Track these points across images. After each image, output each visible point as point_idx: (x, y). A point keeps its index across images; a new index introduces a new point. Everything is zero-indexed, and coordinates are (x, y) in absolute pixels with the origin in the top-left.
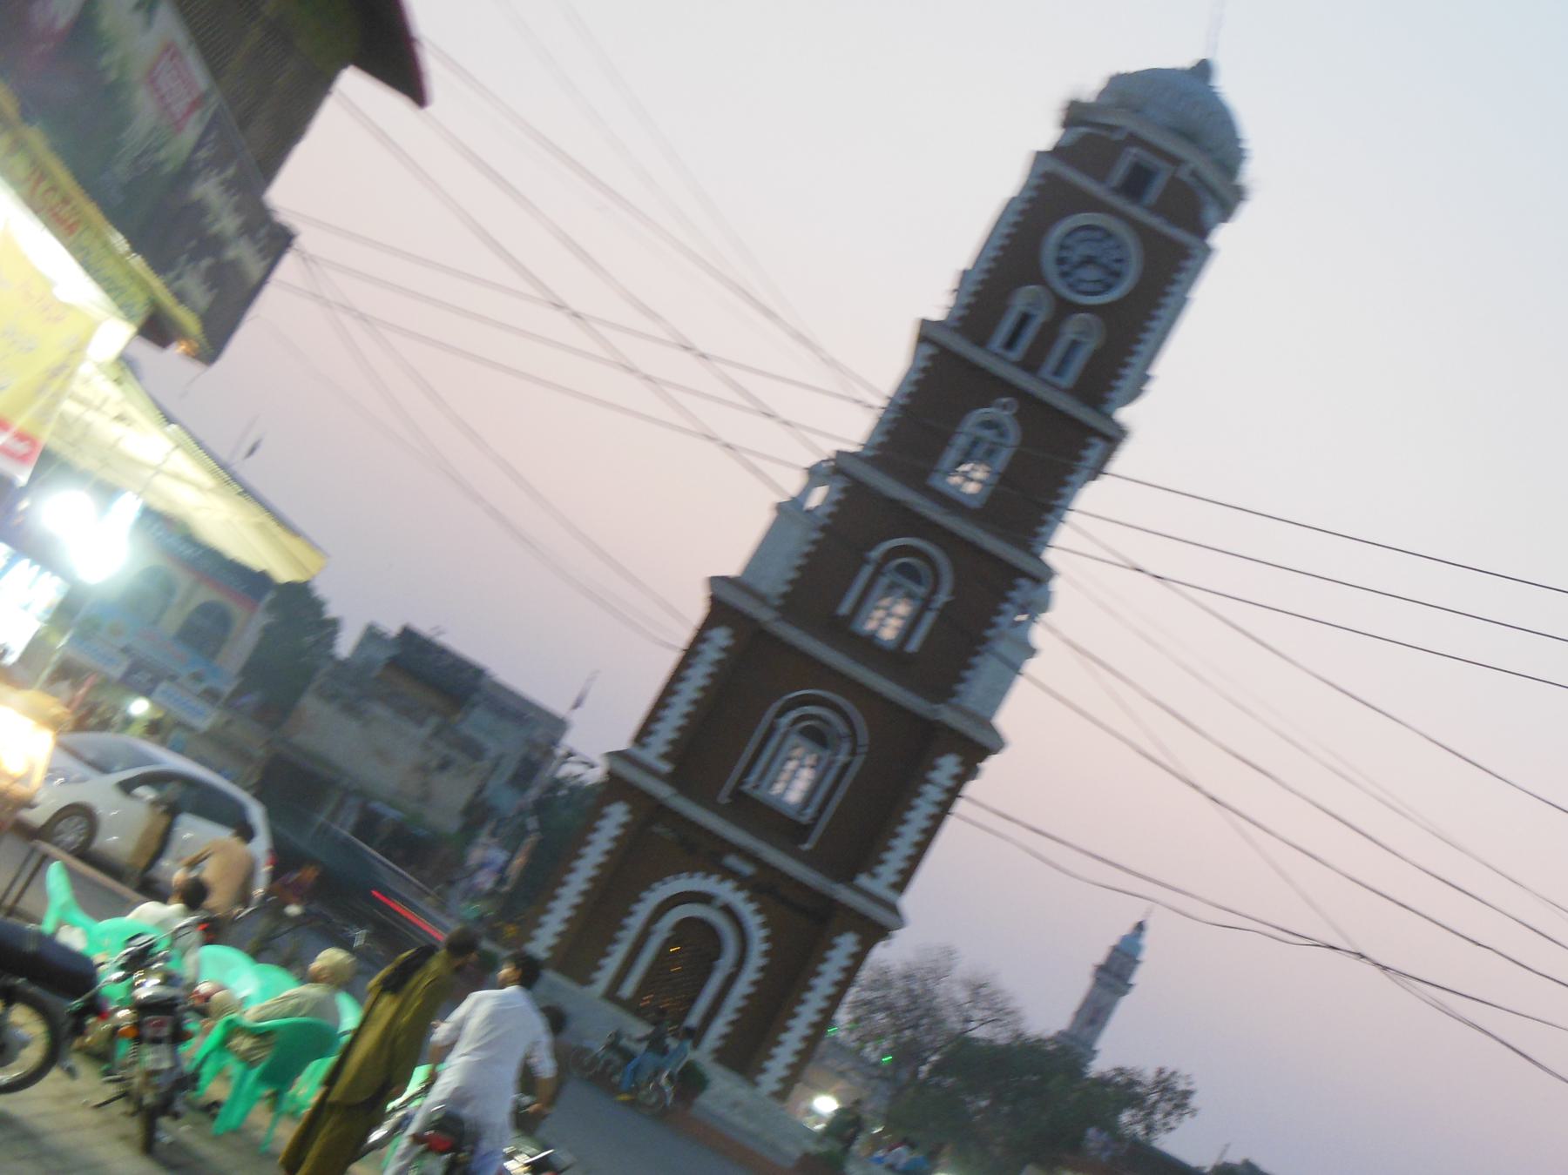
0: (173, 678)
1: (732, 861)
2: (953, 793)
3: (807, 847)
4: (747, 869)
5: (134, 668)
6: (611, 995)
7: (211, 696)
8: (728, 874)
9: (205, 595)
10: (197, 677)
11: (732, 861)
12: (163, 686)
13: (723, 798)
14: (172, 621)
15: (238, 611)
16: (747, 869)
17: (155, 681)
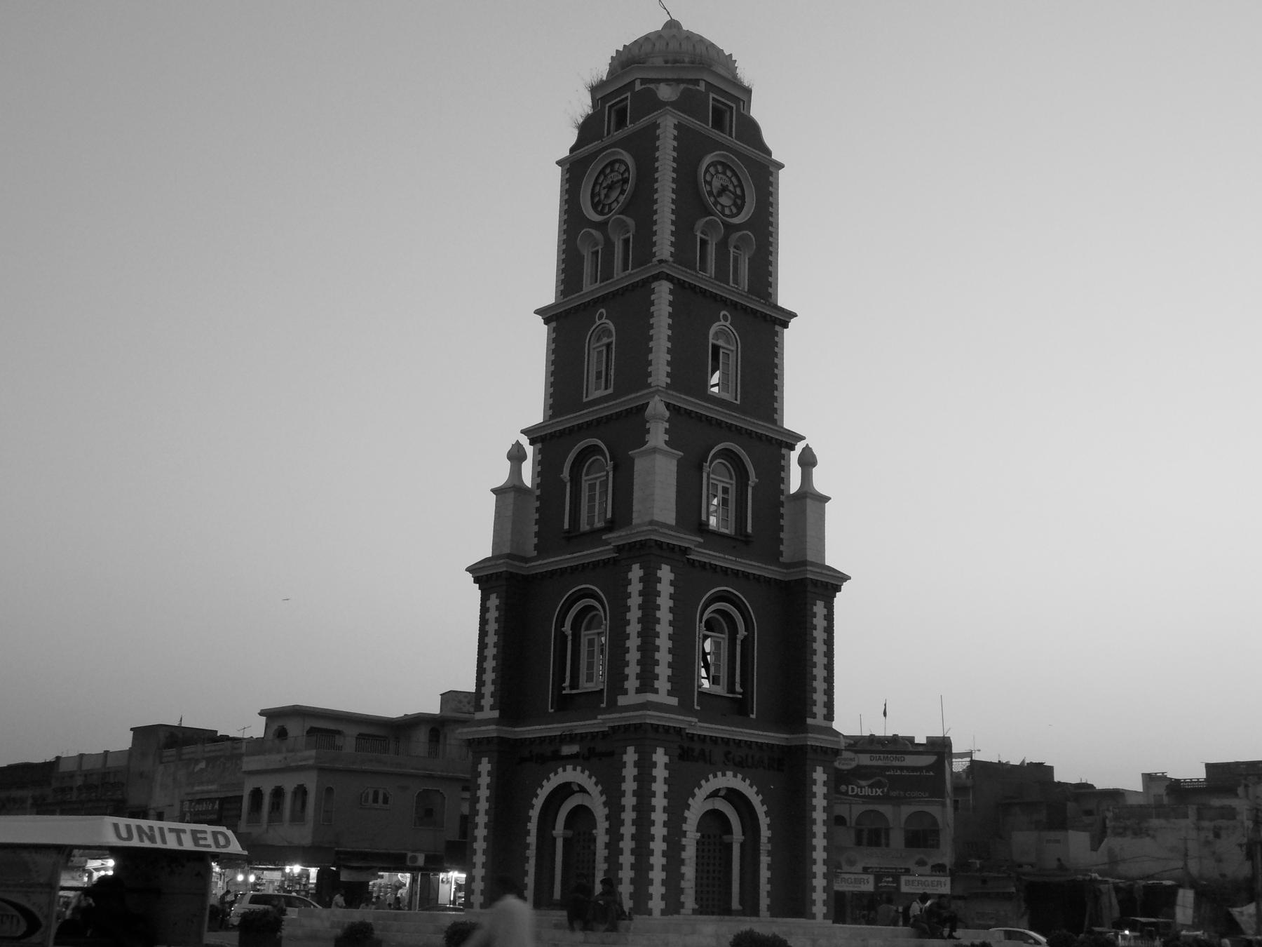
0: (907, 871)
1: (567, 750)
2: (829, 618)
3: (753, 716)
4: (575, 749)
5: (878, 878)
6: (673, 904)
7: (939, 868)
8: (560, 760)
9: (907, 810)
10: (921, 863)
11: (567, 750)
12: (903, 879)
13: (551, 711)
14: (897, 838)
15: (934, 810)
16: (575, 749)
17: (896, 879)
